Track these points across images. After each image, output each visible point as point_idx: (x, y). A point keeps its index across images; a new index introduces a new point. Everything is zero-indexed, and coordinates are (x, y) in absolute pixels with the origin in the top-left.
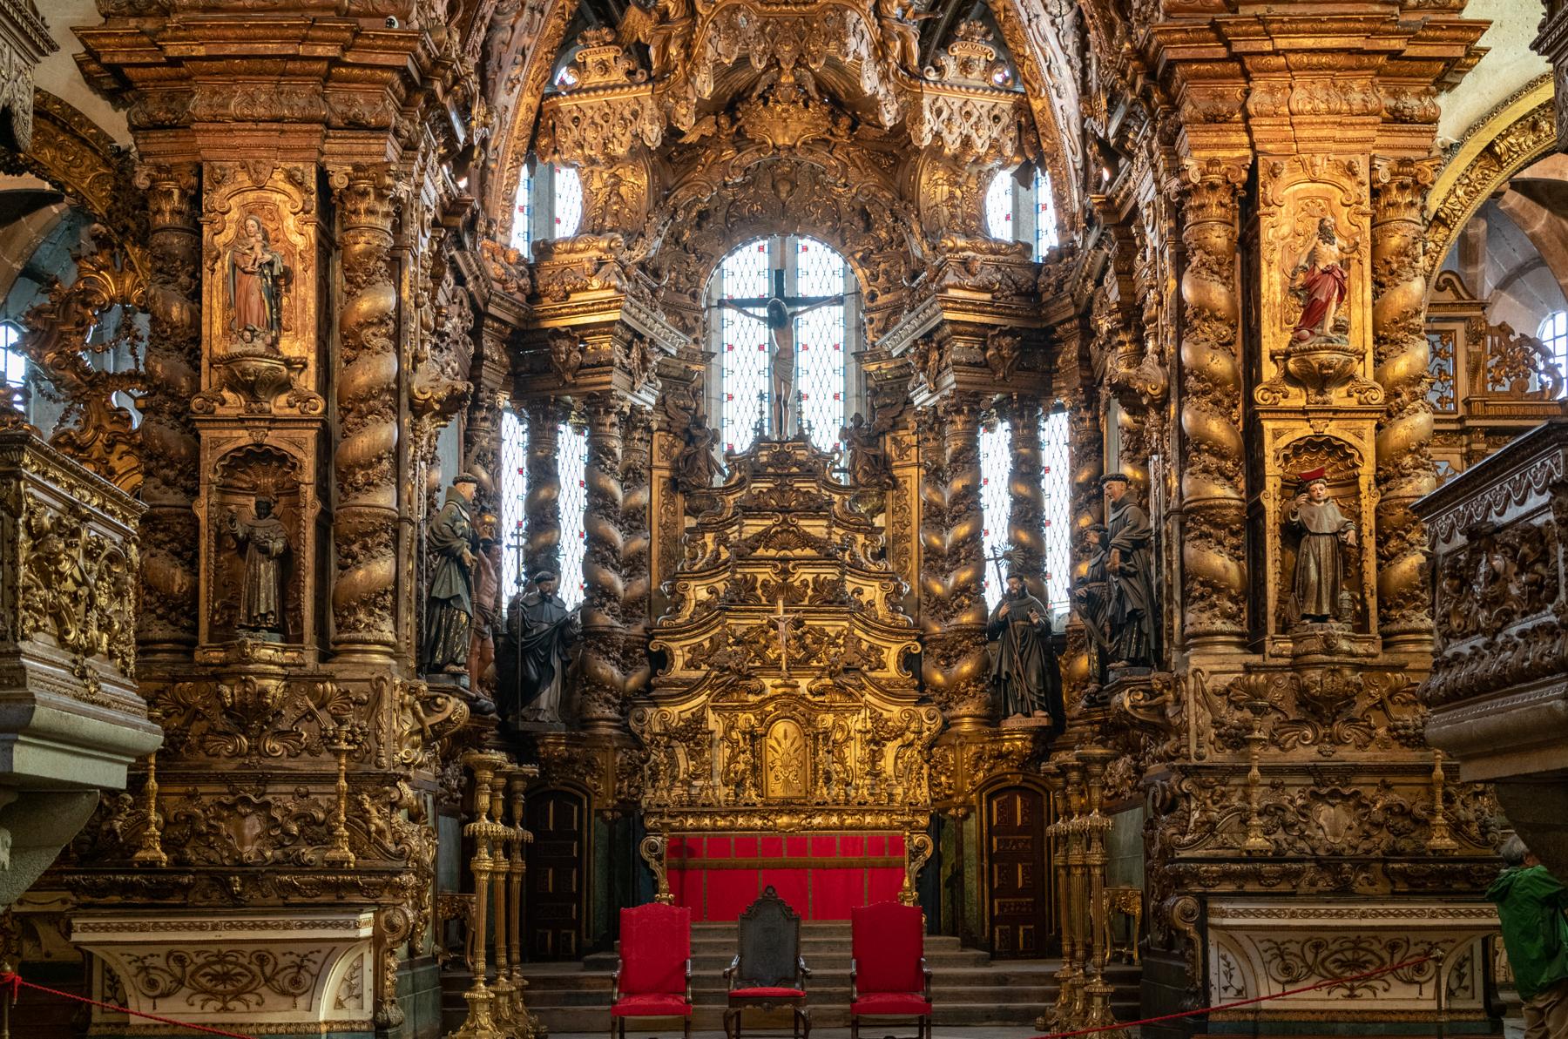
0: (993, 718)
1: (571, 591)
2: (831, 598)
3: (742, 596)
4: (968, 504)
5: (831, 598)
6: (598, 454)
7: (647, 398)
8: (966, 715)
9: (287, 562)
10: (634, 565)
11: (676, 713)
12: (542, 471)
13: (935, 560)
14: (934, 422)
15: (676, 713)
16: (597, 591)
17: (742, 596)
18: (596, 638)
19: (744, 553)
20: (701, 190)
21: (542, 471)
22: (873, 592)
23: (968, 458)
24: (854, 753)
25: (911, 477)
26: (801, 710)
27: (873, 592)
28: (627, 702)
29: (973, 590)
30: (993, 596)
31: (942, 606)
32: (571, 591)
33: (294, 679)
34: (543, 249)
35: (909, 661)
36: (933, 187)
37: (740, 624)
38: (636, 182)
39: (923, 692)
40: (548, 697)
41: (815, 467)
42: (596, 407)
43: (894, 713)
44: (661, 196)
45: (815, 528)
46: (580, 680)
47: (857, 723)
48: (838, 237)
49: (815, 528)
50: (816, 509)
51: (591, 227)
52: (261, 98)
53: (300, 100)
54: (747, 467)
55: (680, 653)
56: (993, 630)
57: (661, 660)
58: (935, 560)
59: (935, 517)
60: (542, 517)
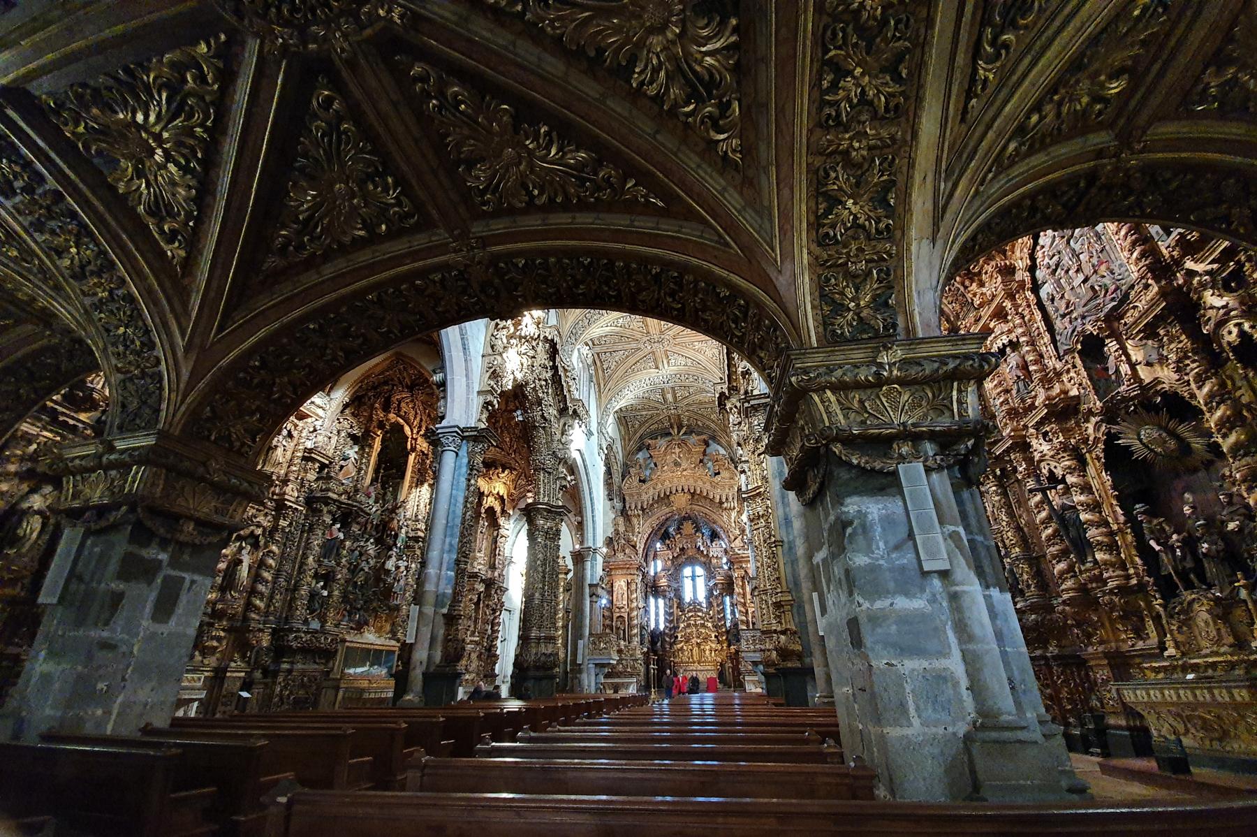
0: (729, 646)
1: (662, 627)
2: (703, 626)
3: (689, 626)
4: (723, 610)
5: (703, 626)
6: (665, 604)
7: (672, 595)
8: (725, 645)
9: (624, 631)
10: (671, 622)
11: (679, 646)
12: (657, 607)
13: (720, 620)
14: (716, 597)
15: (679, 646)
16: (666, 627)
17: (689, 626)
18: (667, 634)
19: (689, 619)
20: (680, 561)
21: (657, 607)
22: (710, 625)
23: (723, 603)
24: (707, 652)
25: (715, 604)
26: (698, 645)
27: (710, 625)
28: (671, 645)
29: (725, 625)
30: (728, 624)
31: (720, 627)
32: (662, 627)
33: (625, 646)
34: (656, 573)
35: (716, 637)
36: (714, 561)
37: (689, 631)
38: (669, 563)
39: (719, 642)
40: (659, 644)
41: (700, 604)
42: (664, 597)
43: (713, 646)
44: (673, 563)
45: (700, 614)
46: (664, 641)
47: (708, 647)
48: (701, 566)
49: (700, 614)
50: (700, 611)
51: (663, 570)
52: (620, 572)
53: (625, 571)
54: (689, 603)
55: (679, 635)
56: (728, 632)
57: (677, 637)
58: (720, 620)
59: (719, 613)
60: (657, 615)
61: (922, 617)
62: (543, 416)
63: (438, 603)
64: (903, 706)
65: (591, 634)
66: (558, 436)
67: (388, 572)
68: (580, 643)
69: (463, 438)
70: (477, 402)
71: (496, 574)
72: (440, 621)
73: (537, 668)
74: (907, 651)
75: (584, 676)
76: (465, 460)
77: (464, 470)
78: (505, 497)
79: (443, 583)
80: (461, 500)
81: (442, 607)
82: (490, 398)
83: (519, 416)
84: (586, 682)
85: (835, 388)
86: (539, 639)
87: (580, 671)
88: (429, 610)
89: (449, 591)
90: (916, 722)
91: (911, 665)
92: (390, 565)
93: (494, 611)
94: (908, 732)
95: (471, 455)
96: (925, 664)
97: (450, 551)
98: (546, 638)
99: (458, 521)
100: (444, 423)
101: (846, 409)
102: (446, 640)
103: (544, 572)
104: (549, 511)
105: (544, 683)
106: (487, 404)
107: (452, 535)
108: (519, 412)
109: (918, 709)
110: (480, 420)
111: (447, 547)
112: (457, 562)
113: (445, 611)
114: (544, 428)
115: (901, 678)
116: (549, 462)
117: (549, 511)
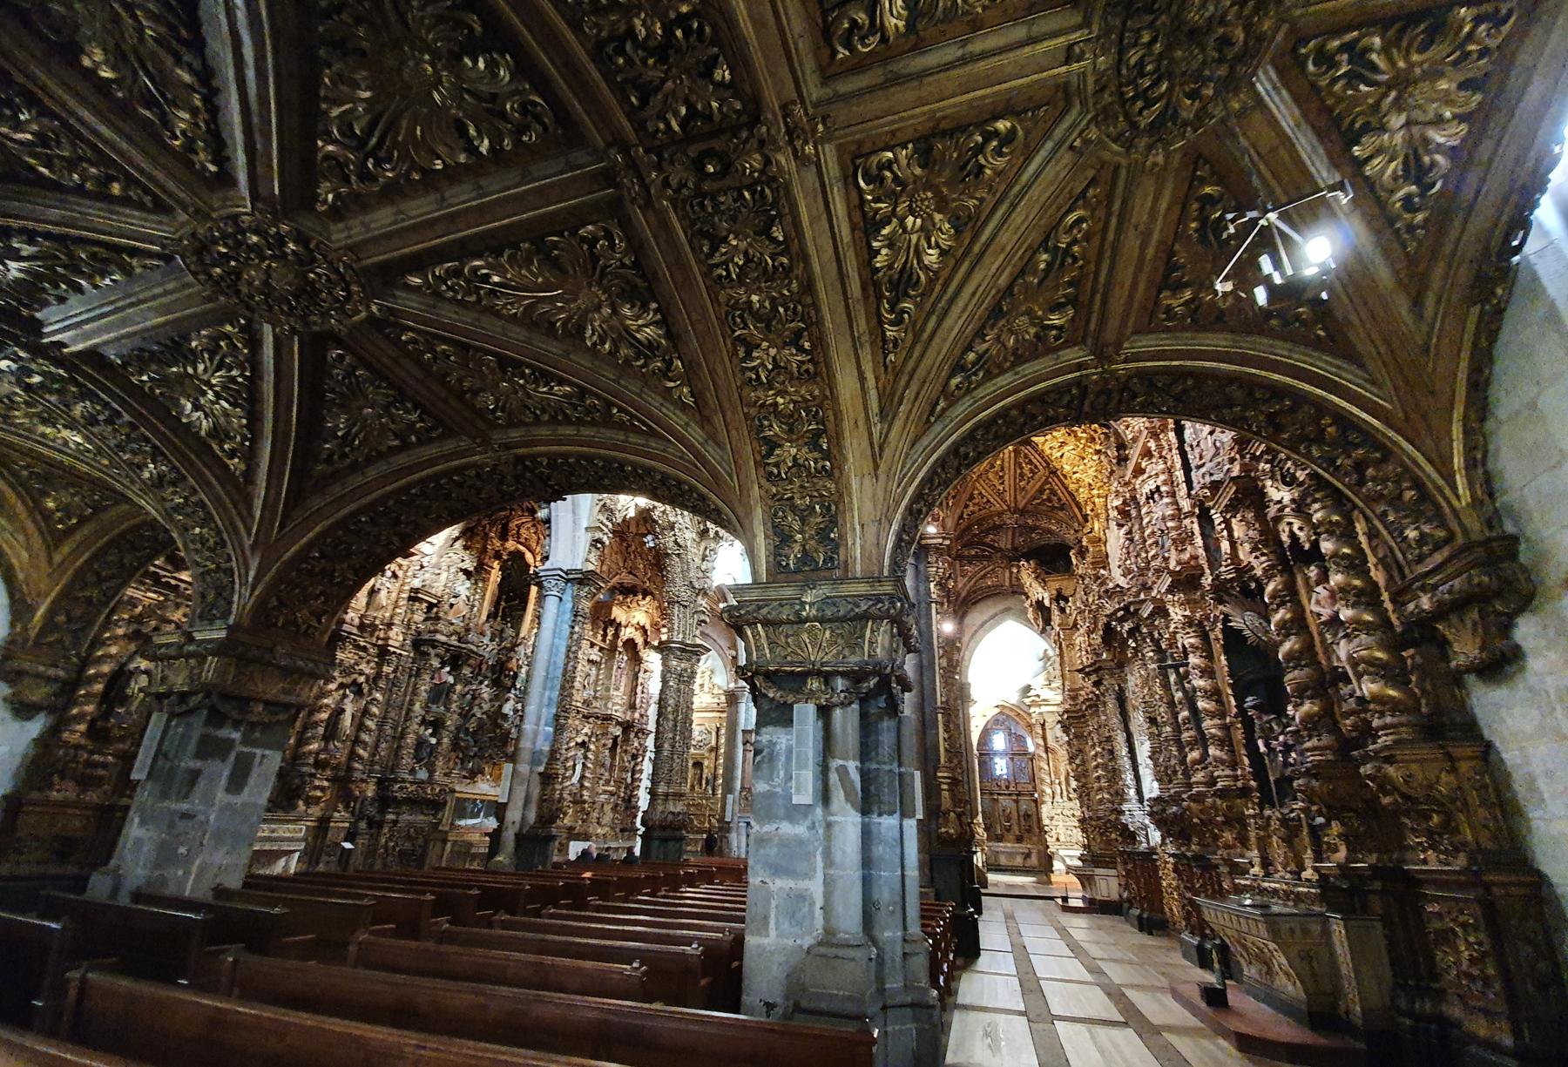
61: (800, 842)
62: (676, 542)
63: (534, 762)
64: (766, 918)
65: (743, 788)
66: (698, 560)
67: (505, 716)
68: (730, 797)
69: (568, 581)
70: (585, 540)
71: (637, 715)
72: (536, 779)
73: (663, 828)
74: (778, 870)
75: (733, 836)
76: (569, 605)
77: (568, 616)
78: (648, 627)
79: (540, 739)
80: (563, 649)
81: (539, 764)
82: (598, 535)
83: (650, 541)
84: (735, 844)
85: (766, 623)
86: (667, 795)
87: (729, 830)
88: (524, 768)
89: (547, 748)
90: (773, 932)
91: (780, 884)
92: (508, 708)
93: (634, 757)
94: (765, 941)
95: (576, 599)
96: (792, 884)
97: (549, 705)
98: (675, 794)
99: (559, 672)
100: (548, 565)
101: (772, 643)
102: (542, 801)
103: (675, 720)
104: (683, 650)
105: (671, 844)
106: (596, 542)
107: (552, 688)
108: (650, 537)
109: (777, 922)
110: (587, 560)
111: (546, 701)
112: (557, 717)
113: (541, 769)
114: (678, 555)
115: (769, 894)
116: (685, 594)
117: (683, 650)
